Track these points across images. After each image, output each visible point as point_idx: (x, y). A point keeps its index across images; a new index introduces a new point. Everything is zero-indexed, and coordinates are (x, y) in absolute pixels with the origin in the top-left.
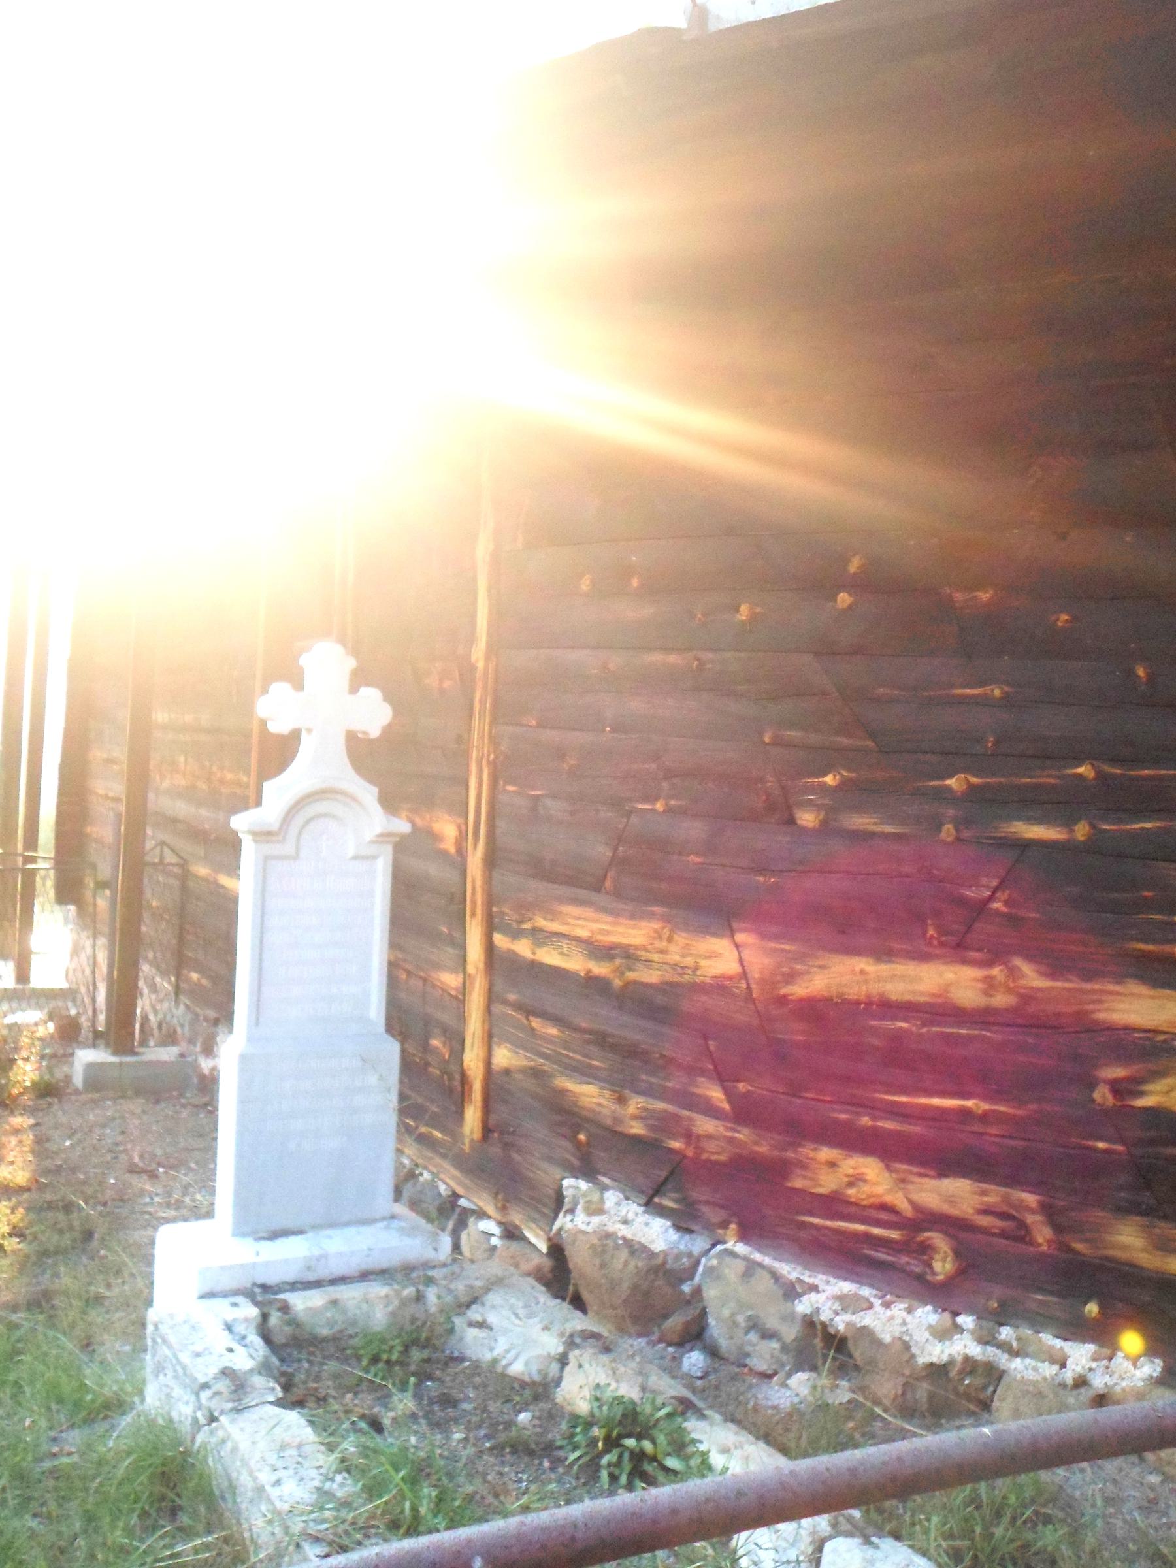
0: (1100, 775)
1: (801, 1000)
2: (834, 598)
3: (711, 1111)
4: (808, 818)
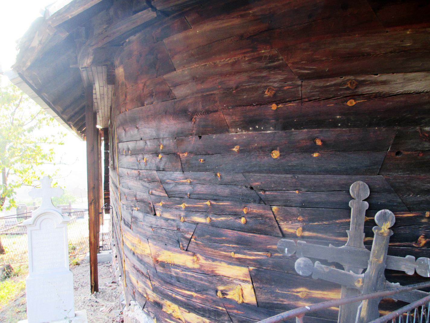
1: (161, 261)
2: (158, 156)
3: (149, 288)
4: (158, 213)
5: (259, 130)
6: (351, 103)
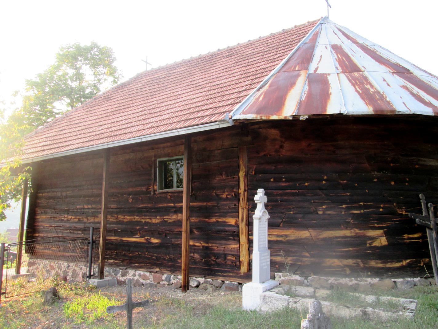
0: (364, 204)
5: (385, 173)
6: (417, 166)
